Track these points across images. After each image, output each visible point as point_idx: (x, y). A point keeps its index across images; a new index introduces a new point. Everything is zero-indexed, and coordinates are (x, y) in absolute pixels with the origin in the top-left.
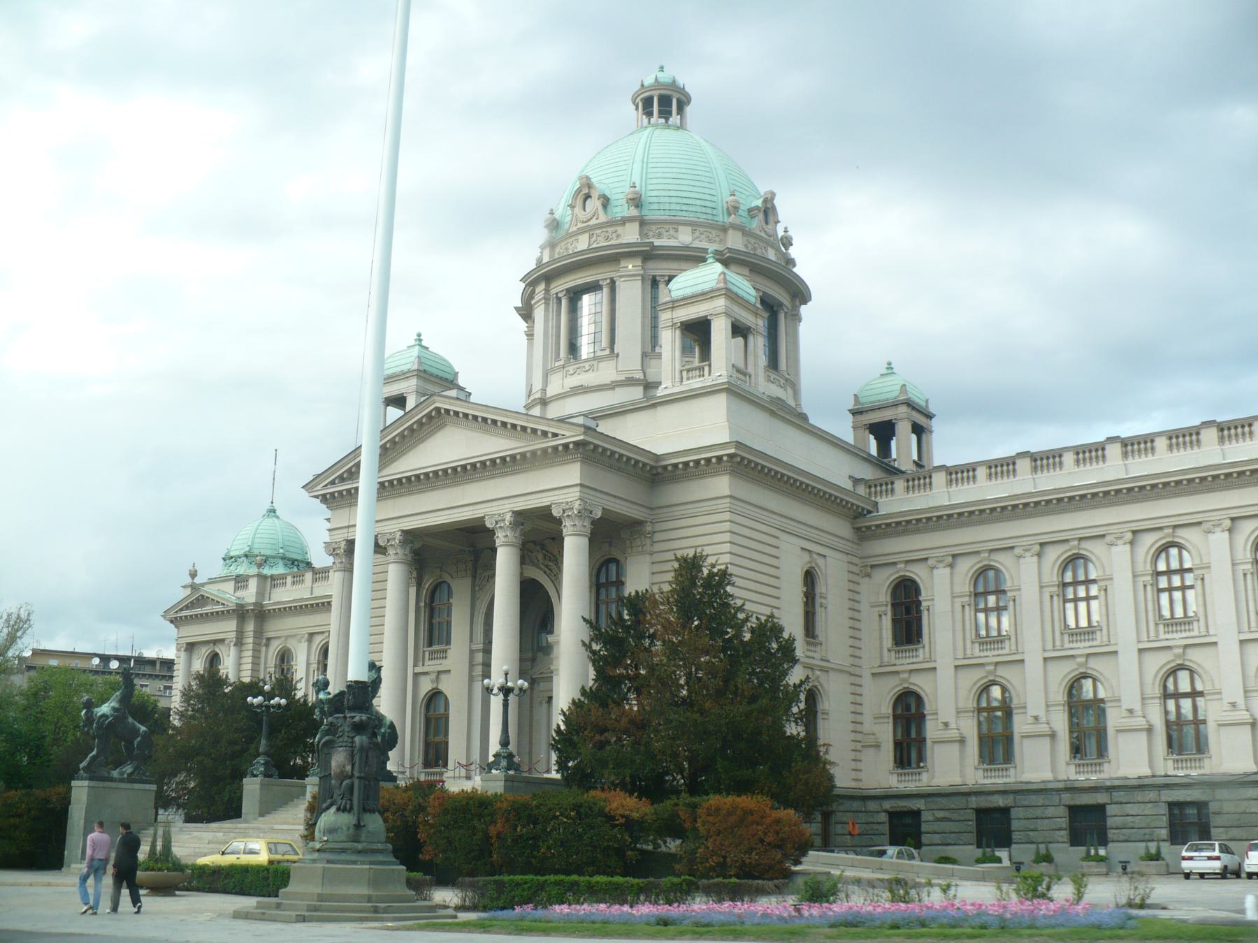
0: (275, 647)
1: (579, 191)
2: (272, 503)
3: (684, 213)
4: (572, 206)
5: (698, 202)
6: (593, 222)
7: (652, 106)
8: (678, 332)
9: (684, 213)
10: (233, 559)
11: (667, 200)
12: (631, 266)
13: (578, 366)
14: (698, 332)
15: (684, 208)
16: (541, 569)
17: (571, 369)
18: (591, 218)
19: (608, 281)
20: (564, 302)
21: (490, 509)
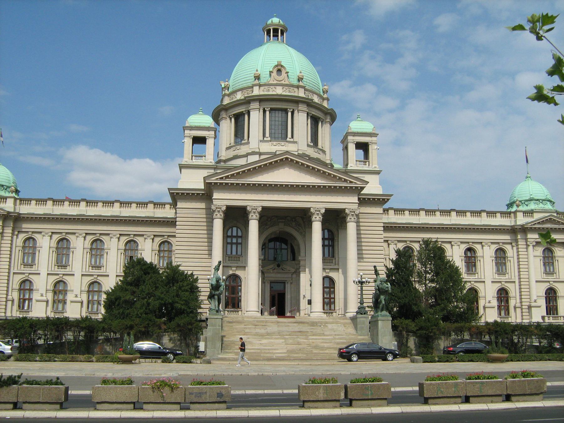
0: (22, 237)
1: (276, 66)
3: (314, 89)
4: (271, 72)
5: (316, 85)
6: (283, 82)
7: (278, 33)
8: (355, 145)
9: (314, 89)
11: (308, 81)
12: (302, 107)
13: (279, 142)
14: (363, 147)
15: (314, 87)
16: (294, 228)
17: (275, 143)
18: (282, 80)
19: (292, 110)
20: (268, 113)
21: (312, 205)
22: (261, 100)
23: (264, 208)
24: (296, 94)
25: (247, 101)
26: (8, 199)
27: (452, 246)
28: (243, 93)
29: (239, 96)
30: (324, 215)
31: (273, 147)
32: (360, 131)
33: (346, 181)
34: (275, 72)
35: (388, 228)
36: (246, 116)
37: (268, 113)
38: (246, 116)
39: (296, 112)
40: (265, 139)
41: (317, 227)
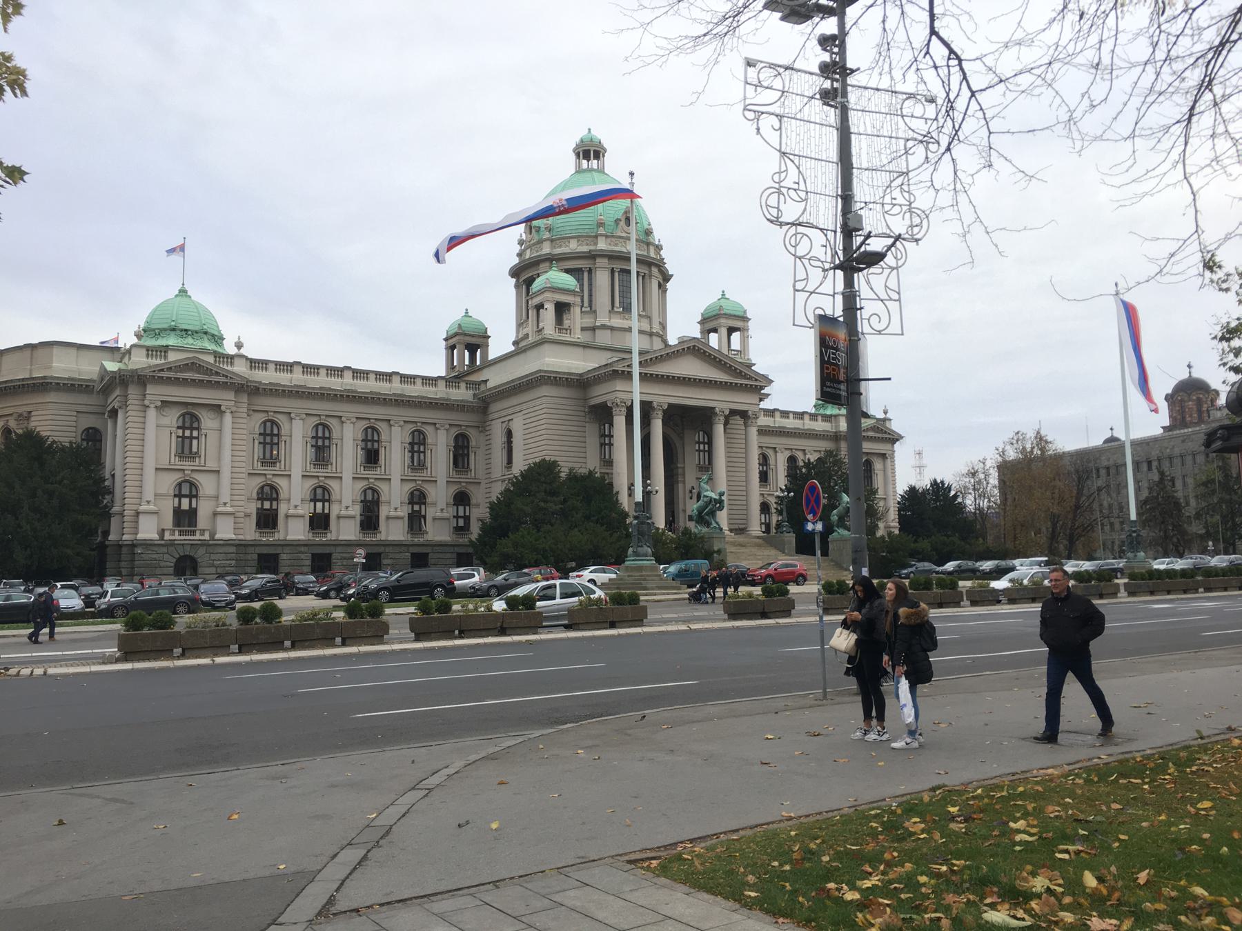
2: (183, 284)
10: (190, 333)
22: (612, 257)
23: (670, 405)
24: (645, 253)
25: (592, 256)
26: (236, 359)
27: (391, 426)
28: (580, 242)
29: (573, 246)
30: (664, 411)
31: (625, 321)
32: (732, 313)
33: (750, 378)
34: (623, 220)
35: (763, 431)
36: (586, 274)
37: (616, 275)
38: (586, 274)
39: (647, 277)
40: (616, 309)
41: (719, 429)
